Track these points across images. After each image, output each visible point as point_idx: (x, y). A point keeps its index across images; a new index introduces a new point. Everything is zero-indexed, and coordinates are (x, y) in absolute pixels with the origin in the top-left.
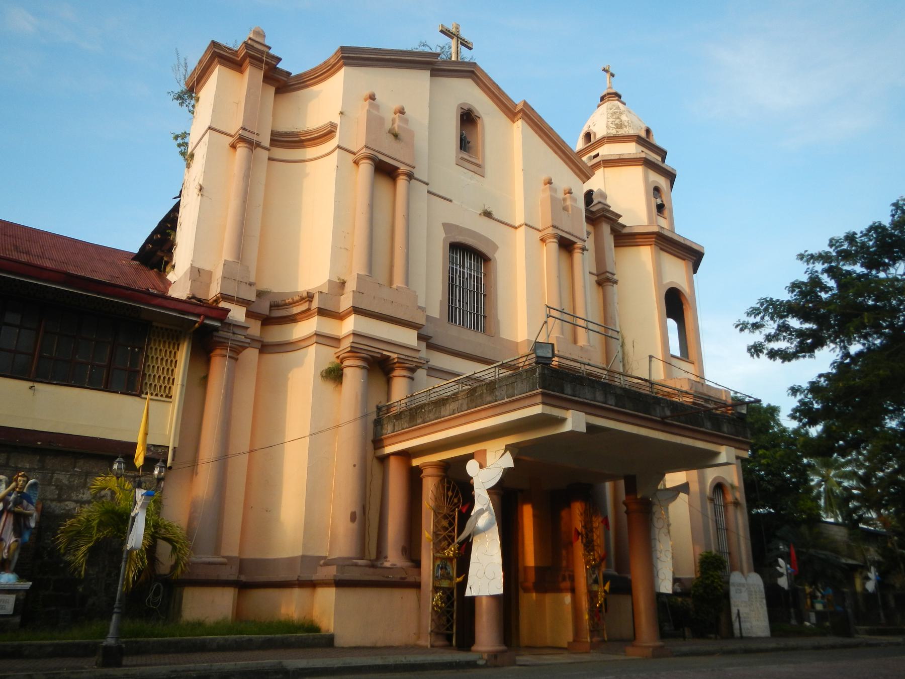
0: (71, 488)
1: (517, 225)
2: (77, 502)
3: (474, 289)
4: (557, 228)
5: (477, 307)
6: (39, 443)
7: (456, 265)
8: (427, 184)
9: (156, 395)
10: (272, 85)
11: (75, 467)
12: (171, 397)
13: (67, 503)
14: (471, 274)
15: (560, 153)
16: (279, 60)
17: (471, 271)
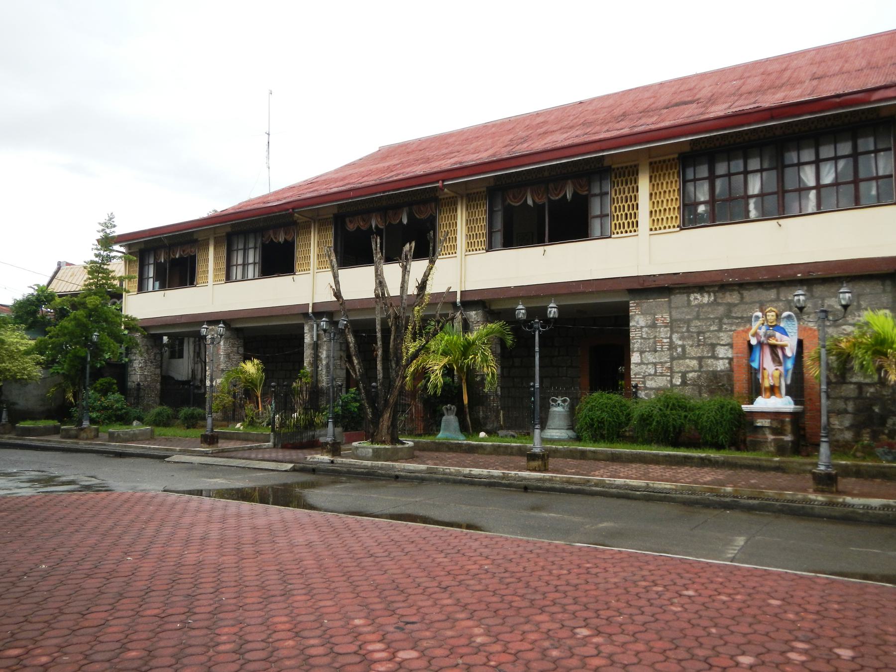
2: (854, 325)
6: (799, 275)
13: (844, 327)
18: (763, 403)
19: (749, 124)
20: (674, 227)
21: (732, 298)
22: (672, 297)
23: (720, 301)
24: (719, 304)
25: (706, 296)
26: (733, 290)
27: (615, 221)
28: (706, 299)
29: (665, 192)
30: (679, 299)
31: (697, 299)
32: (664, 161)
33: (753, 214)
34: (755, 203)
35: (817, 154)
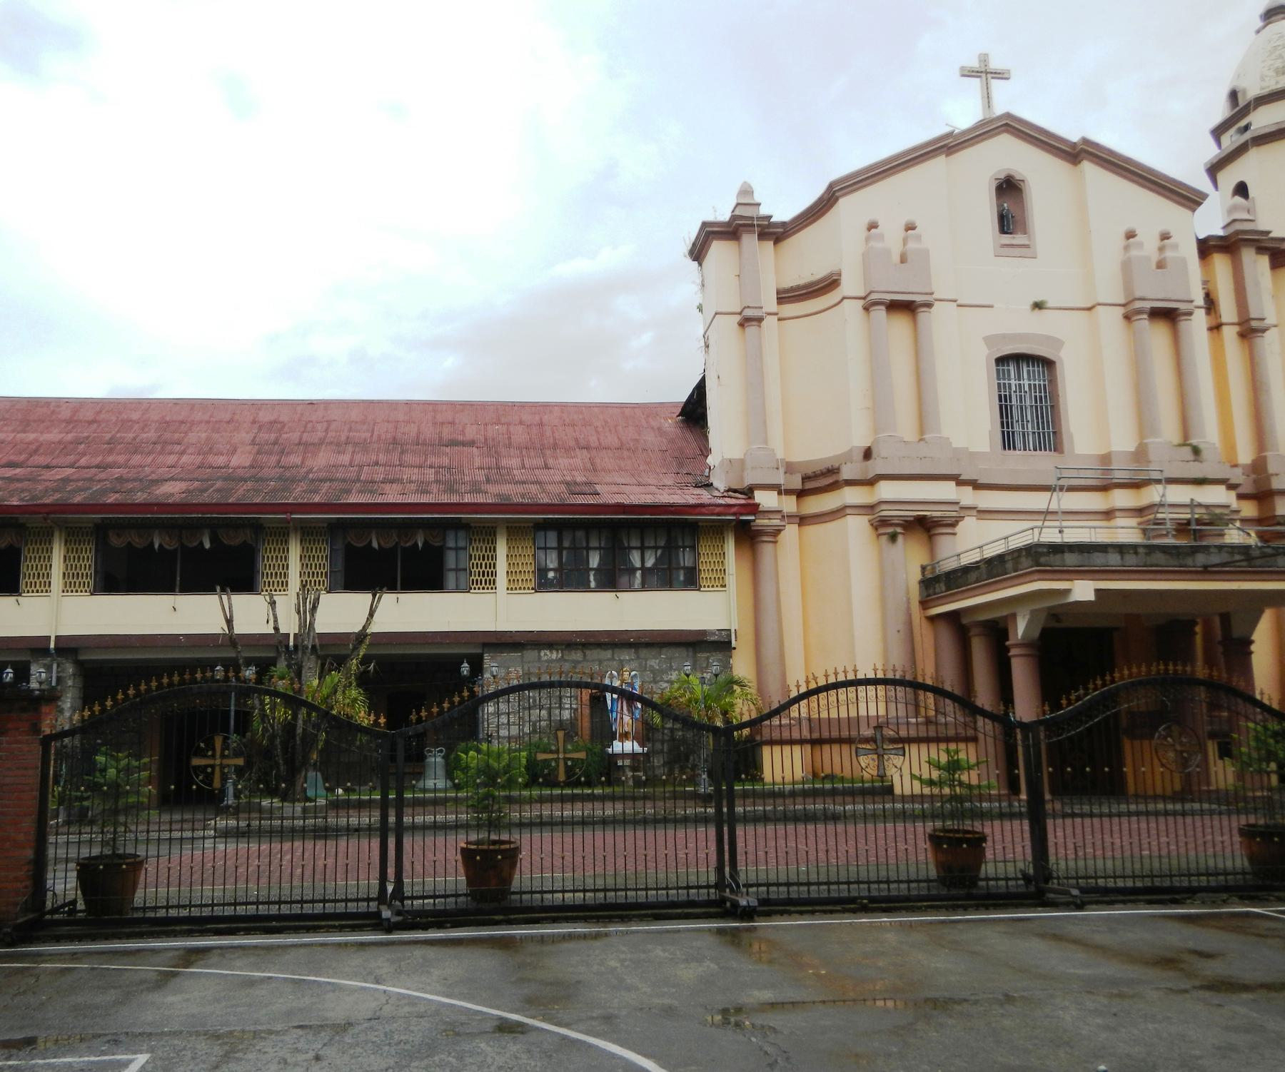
0: (662, 672)
1: (1089, 305)
2: (667, 682)
3: (1036, 402)
4: (1144, 299)
5: (1043, 423)
7: (1009, 380)
8: (955, 301)
9: (713, 586)
10: (769, 240)
11: (660, 655)
12: (725, 586)
14: (1030, 385)
15: (1148, 184)
16: (771, 217)
17: (1029, 380)
18: (617, 747)
19: (605, 514)
20: (528, 588)
21: (577, 655)
22: (525, 652)
23: (566, 658)
24: (566, 661)
25: (555, 652)
26: (577, 649)
27: (473, 577)
28: (554, 655)
29: (520, 555)
30: (530, 654)
31: (546, 655)
32: (520, 527)
33: (593, 584)
34: (594, 575)
35: (642, 543)
